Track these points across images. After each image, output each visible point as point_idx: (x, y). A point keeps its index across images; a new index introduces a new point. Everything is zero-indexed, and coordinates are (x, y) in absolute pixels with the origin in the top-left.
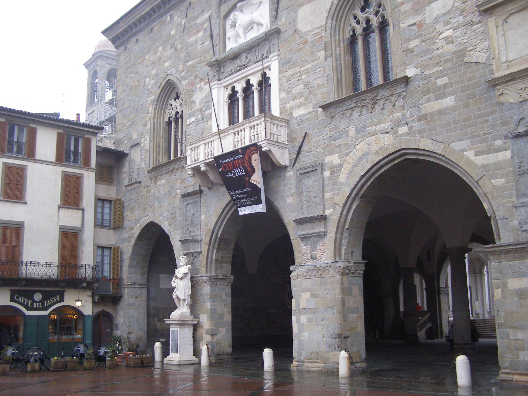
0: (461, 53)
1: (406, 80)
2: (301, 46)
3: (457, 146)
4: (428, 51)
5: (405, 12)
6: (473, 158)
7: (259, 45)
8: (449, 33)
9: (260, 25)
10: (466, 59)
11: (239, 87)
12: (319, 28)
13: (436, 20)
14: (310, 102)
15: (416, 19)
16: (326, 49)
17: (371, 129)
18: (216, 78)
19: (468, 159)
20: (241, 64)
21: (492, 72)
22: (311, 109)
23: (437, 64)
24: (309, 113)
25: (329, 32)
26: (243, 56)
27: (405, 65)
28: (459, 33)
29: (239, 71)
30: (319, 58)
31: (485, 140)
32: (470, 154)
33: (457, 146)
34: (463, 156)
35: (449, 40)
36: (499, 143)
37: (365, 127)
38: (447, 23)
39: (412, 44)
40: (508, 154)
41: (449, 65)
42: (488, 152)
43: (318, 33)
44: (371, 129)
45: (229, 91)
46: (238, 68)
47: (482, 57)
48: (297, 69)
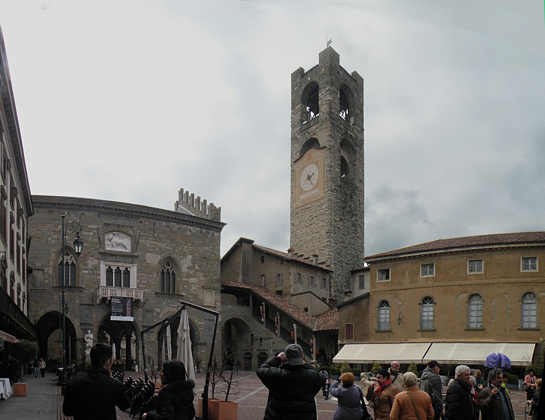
0: (197, 295)
1: (183, 296)
2: (147, 267)
3: (194, 317)
4: (189, 290)
5: (184, 276)
6: (197, 321)
7: (127, 256)
8: (195, 288)
9: (127, 249)
10: (198, 297)
11: (114, 268)
12: (155, 265)
13: (192, 283)
14: (150, 288)
15: (187, 280)
16: (157, 274)
17: (171, 305)
18: (103, 259)
19: (196, 322)
20: (116, 259)
21: (203, 303)
22: (150, 291)
23: (191, 295)
24: (149, 292)
25: (159, 268)
26: (118, 257)
27: (183, 292)
28: (197, 289)
29: (115, 262)
30: (154, 275)
31: (200, 318)
32: (196, 320)
33: (194, 317)
34: (194, 321)
35: (194, 290)
36: (202, 320)
37: (169, 304)
38: (194, 285)
39: (185, 286)
40: (204, 323)
41: (194, 296)
42: (200, 321)
43: (154, 267)
44: (171, 305)
45: (107, 267)
46: (114, 261)
47: (202, 299)
48: (145, 275)
